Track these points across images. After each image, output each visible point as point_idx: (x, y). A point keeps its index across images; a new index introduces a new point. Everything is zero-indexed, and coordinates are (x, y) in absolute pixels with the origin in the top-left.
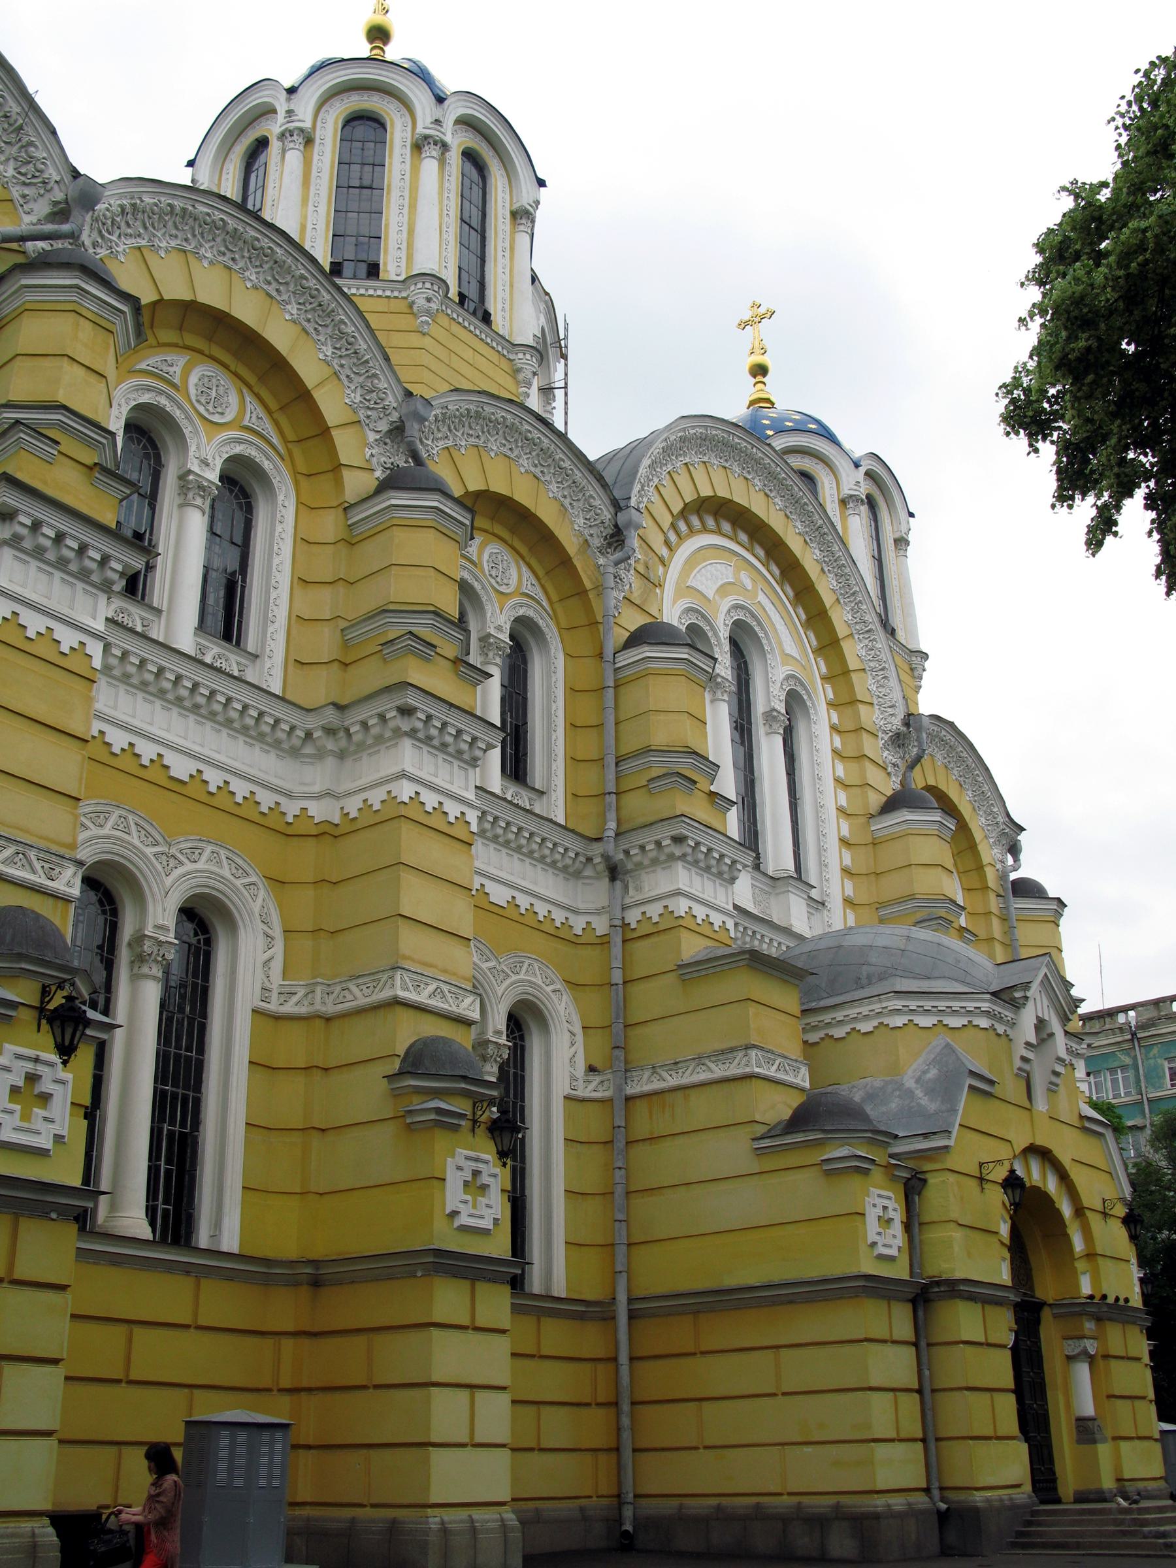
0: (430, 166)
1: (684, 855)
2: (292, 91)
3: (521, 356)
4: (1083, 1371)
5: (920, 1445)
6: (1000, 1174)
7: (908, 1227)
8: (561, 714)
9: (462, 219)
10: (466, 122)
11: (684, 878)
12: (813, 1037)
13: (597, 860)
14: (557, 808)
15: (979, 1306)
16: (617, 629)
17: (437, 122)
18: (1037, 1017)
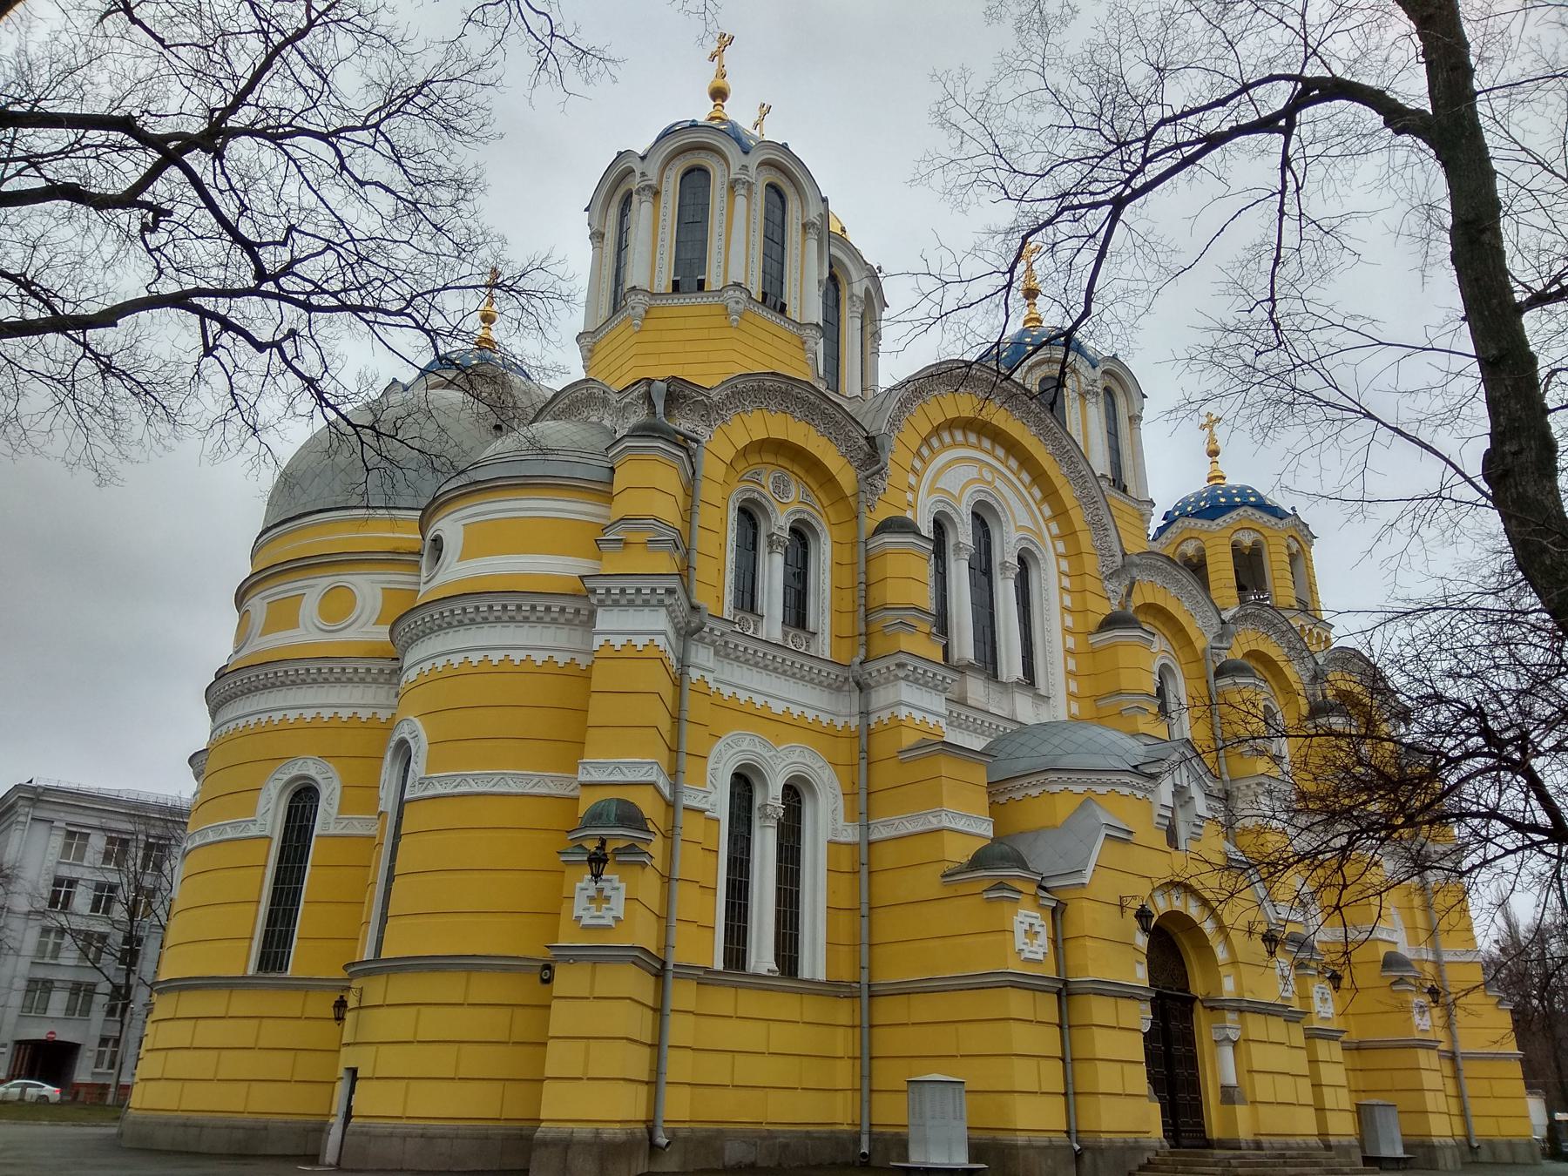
0: (741, 202)
1: (907, 676)
2: (643, 158)
3: (808, 331)
4: (1228, 1051)
5: (1062, 1099)
6: (1136, 905)
7: (1054, 941)
8: (828, 581)
9: (765, 236)
10: (768, 164)
11: (907, 693)
12: (1002, 799)
13: (851, 679)
14: (824, 646)
15: (1112, 1000)
16: (868, 521)
17: (745, 167)
18: (1175, 785)
